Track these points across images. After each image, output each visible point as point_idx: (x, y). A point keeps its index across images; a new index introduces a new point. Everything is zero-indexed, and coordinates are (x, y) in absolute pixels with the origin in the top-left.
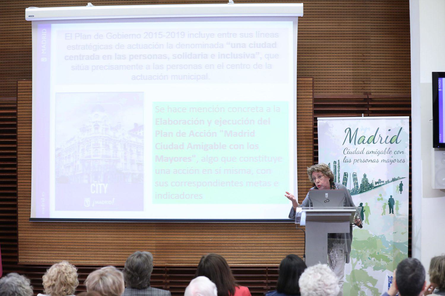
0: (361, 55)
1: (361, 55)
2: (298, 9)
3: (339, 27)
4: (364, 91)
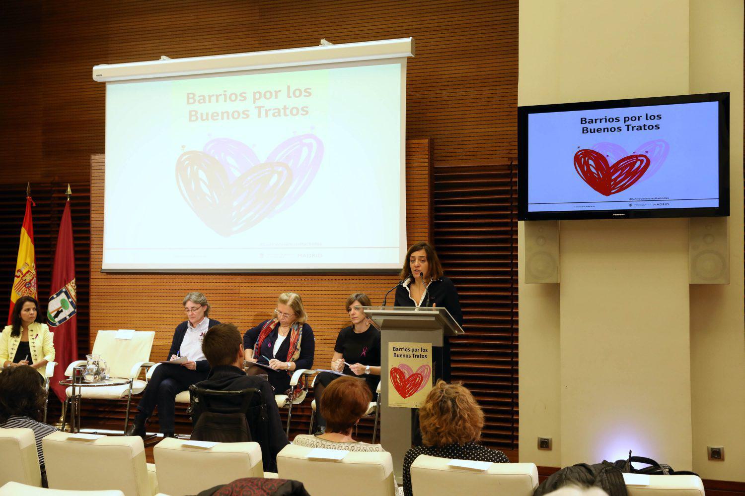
0: (506, 106)
1: (506, 106)
2: (403, 45)
3: (478, 70)
4: (508, 156)
